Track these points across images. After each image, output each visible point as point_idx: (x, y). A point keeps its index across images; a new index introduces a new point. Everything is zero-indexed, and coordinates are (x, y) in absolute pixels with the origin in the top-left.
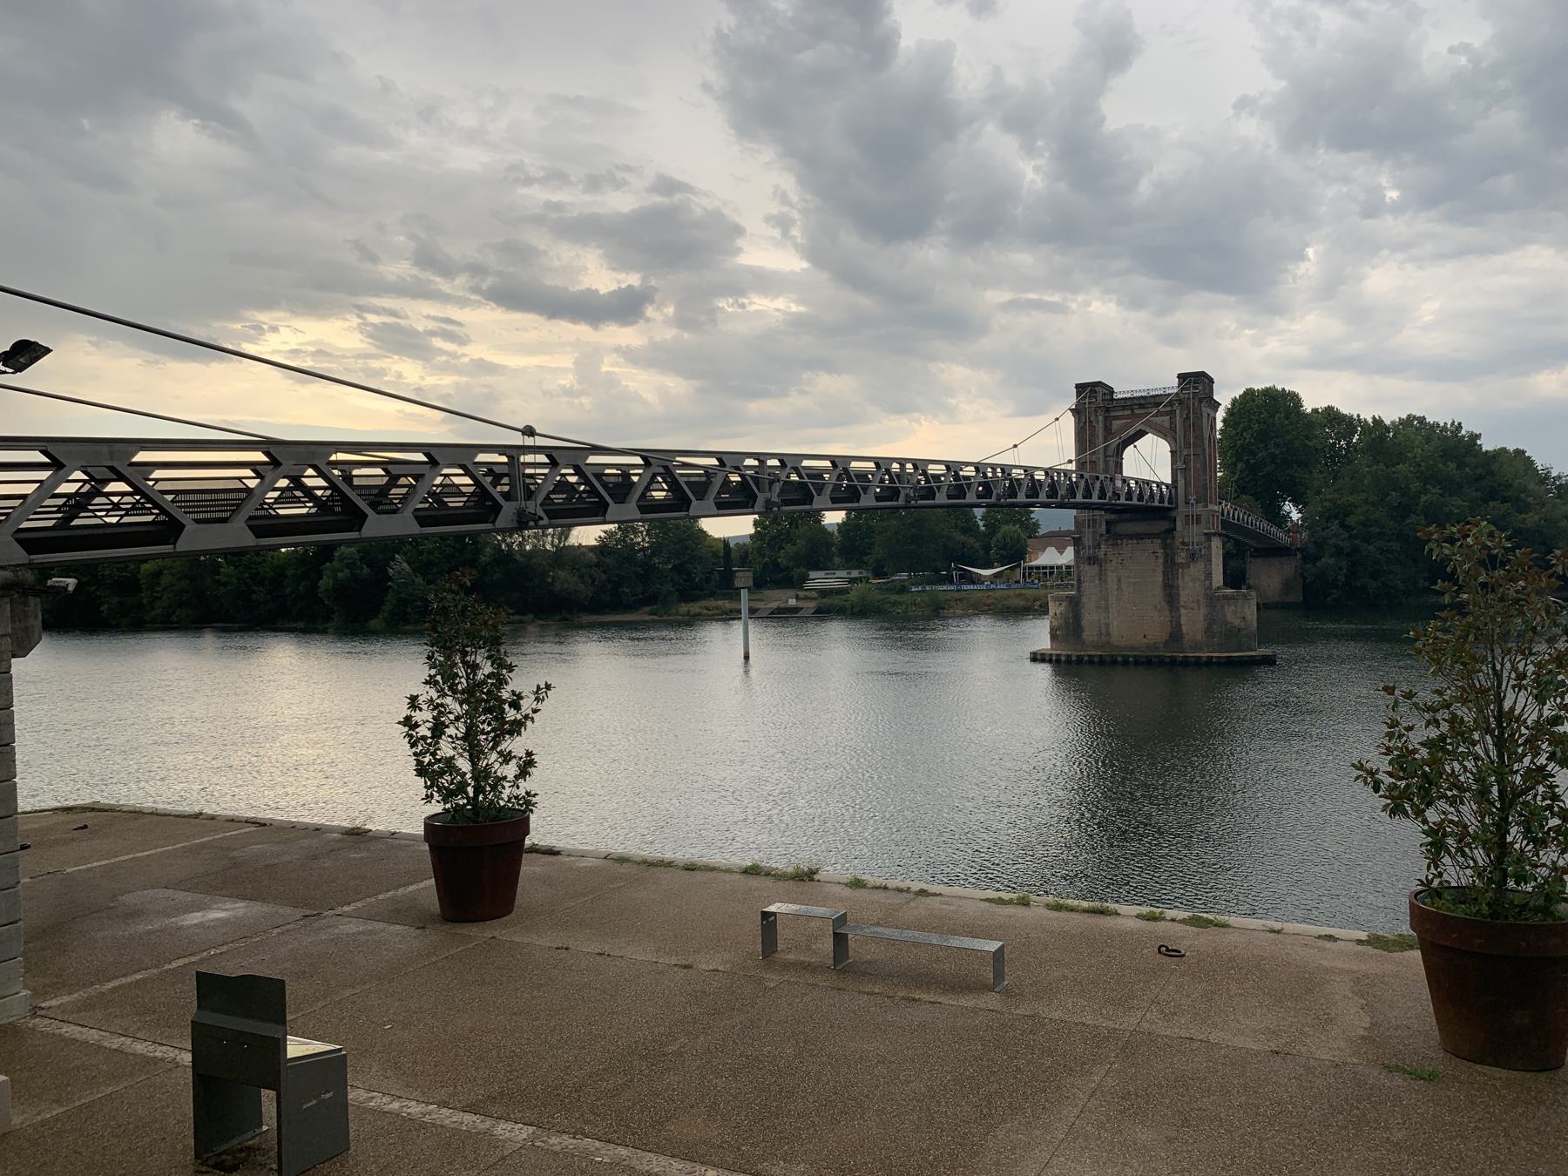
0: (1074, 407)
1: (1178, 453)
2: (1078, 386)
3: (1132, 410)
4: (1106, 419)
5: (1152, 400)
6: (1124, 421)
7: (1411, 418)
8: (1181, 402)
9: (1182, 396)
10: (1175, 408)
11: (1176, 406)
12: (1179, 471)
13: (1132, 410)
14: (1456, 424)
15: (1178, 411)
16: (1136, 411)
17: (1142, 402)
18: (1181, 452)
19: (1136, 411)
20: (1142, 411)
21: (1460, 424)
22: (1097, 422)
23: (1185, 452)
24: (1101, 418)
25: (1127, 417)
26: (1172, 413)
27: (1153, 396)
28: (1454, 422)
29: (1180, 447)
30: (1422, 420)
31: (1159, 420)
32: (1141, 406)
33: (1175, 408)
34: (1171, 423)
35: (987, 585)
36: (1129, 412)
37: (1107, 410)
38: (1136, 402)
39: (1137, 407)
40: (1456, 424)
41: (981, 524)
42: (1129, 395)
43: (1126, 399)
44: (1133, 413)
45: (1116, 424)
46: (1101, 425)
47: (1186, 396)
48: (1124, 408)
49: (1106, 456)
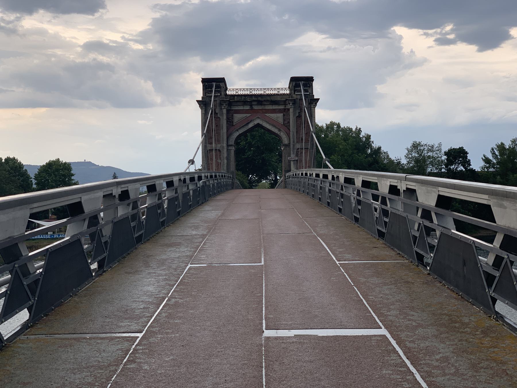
0: (201, 99)
1: (291, 146)
2: (204, 81)
3: (251, 106)
4: (228, 111)
5: (268, 98)
6: (245, 115)
7: (332, 124)
8: (294, 102)
9: (295, 97)
10: (288, 107)
11: (290, 106)
12: (292, 163)
13: (251, 106)
14: (358, 129)
15: (291, 110)
16: (255, 107)
17: (260, 99)
18: (294, 145)
19: (255, 107)
20: (260, 107)
21: (360, 129)
22: (222, 114)
23: (298, 146)
24: (225, 111)
25: (246, 112)
26: (286, 111)
27: (268, 95)
28: (357, 128)
29: (294, 142)
30: (338, 125)
31: (273, 116)
32: (260, 103)
33: (288, 107)
34: (284, 120)
35: (51, 235)
36: (247, 108)
37: (230, 104)
38: (254, 98)
39: (254, 103)
40: (358, 129)
41: (34, 181)
42: (248, 93)
43: (245, 96)
44: (252, 109)
45: (237, 117)
46: (225, 117)
47: (299, 97)
48: (245, 103)
49: (228, 146)
